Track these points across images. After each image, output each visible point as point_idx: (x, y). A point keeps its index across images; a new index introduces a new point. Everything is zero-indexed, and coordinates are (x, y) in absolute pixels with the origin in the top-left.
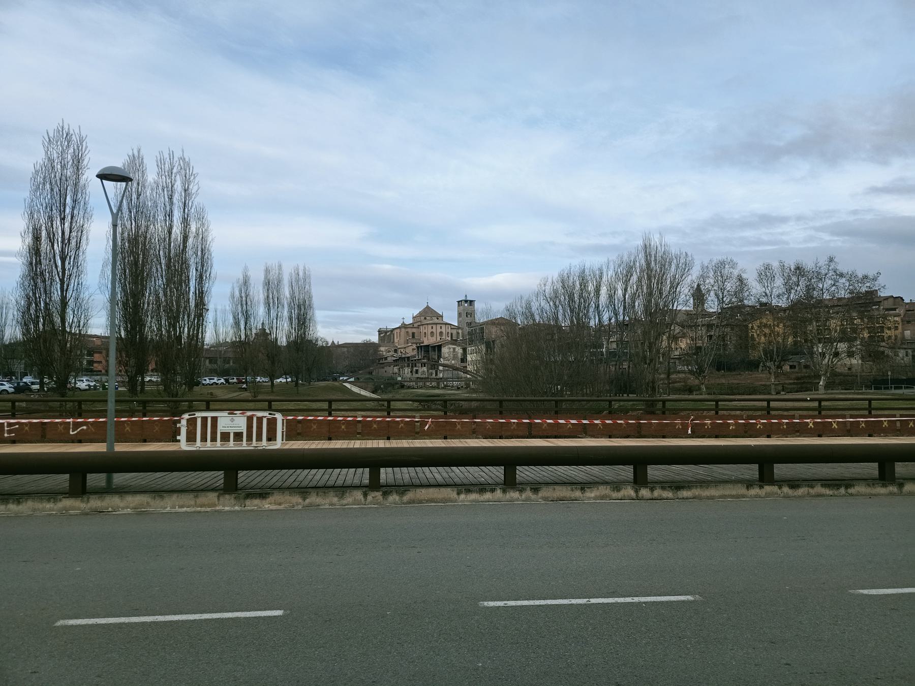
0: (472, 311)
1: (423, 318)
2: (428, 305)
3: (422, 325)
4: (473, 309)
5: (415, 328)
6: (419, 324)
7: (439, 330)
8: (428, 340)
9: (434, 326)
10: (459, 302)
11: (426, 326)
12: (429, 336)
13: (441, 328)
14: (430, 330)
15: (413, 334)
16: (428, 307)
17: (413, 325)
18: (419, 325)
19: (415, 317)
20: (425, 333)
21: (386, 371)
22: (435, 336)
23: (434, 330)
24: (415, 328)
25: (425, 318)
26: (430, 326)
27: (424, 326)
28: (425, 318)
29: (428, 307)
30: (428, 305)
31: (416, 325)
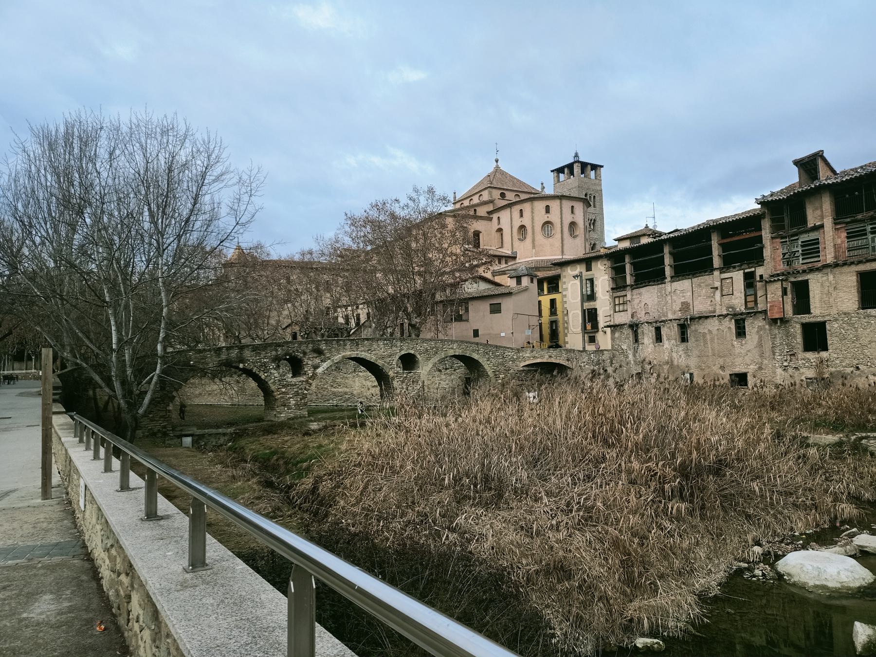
0: (597, 191)
1: (496, 194)
2: (497, 167)
3: (510, 205)
4: (598, 188)
5: (482, 218)
6: (490, 208)
7: (568, 218)
8: (534, 247)
9: (555, 205)
10: (560, 170)
11: (526, 207)
12: (539, 237)
13: (572, 212)
14: (541, 217)
15: (477, 234)
16: (497, 169)
17: (475, 210)
18: (489, 213)
19: (469, 197)
20: (522, 227)
21: (476, 333)
22: (559, 236)
23: (554, 217)
24: (482, 218)
25: (503, 195)
26: (540, 206)
27: (516, 209)
28: (503, 195)
29: (497, 169)
30: (497, 167)
31: (482, 211)
